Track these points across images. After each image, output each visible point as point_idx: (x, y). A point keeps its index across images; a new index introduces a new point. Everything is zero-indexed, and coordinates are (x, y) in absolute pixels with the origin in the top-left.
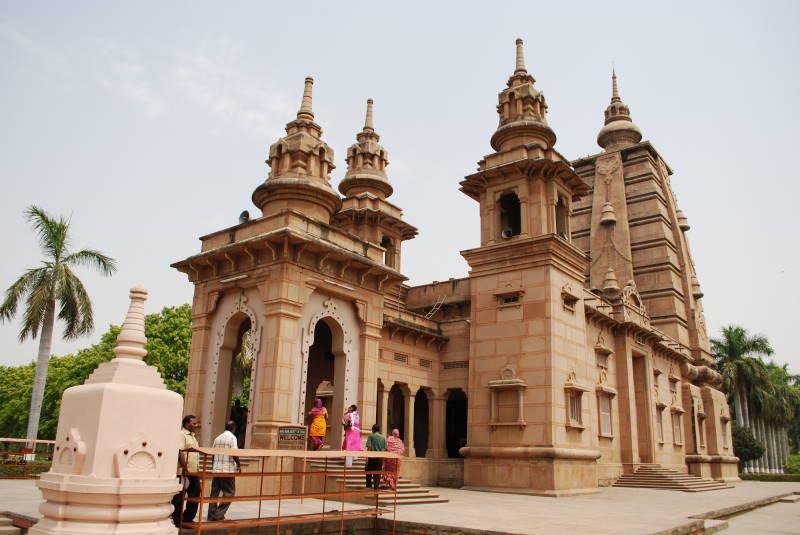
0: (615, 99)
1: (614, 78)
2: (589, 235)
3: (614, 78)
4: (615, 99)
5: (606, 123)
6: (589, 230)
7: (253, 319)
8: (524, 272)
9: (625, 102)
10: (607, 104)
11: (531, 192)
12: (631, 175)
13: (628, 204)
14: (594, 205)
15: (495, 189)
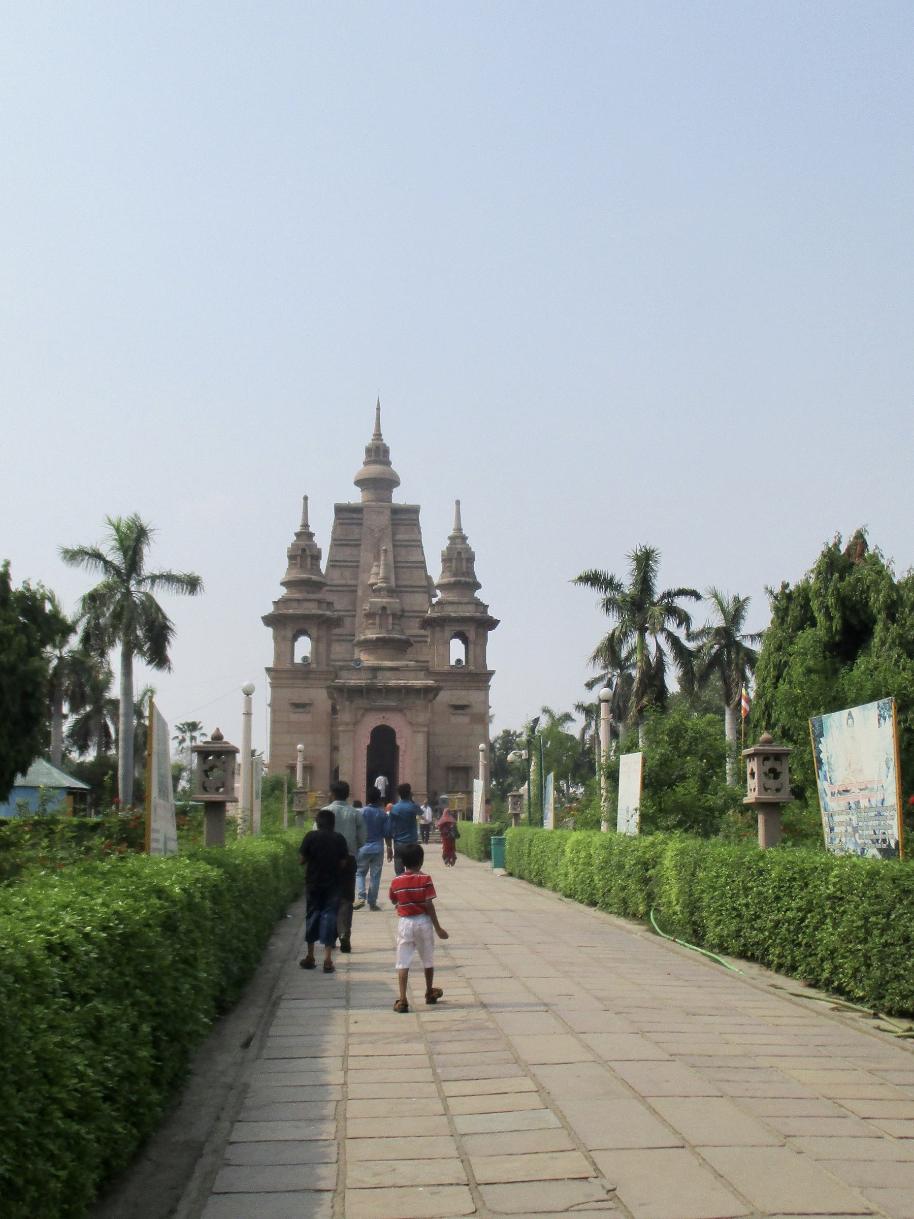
0: (378, 435)
1: (378, 409)
2: (356, 591)
3: (378, 409)
4: (378, 435)
5: (366, 463)
6: (357, 586)
7: (396, 730)
8: (471, 692)
9: (387, 440)
10: (368, 439)
11: (477, 634)
12: (399, 537)
13: (395, 567)
14: (361, 560)
15: (452, 628)
